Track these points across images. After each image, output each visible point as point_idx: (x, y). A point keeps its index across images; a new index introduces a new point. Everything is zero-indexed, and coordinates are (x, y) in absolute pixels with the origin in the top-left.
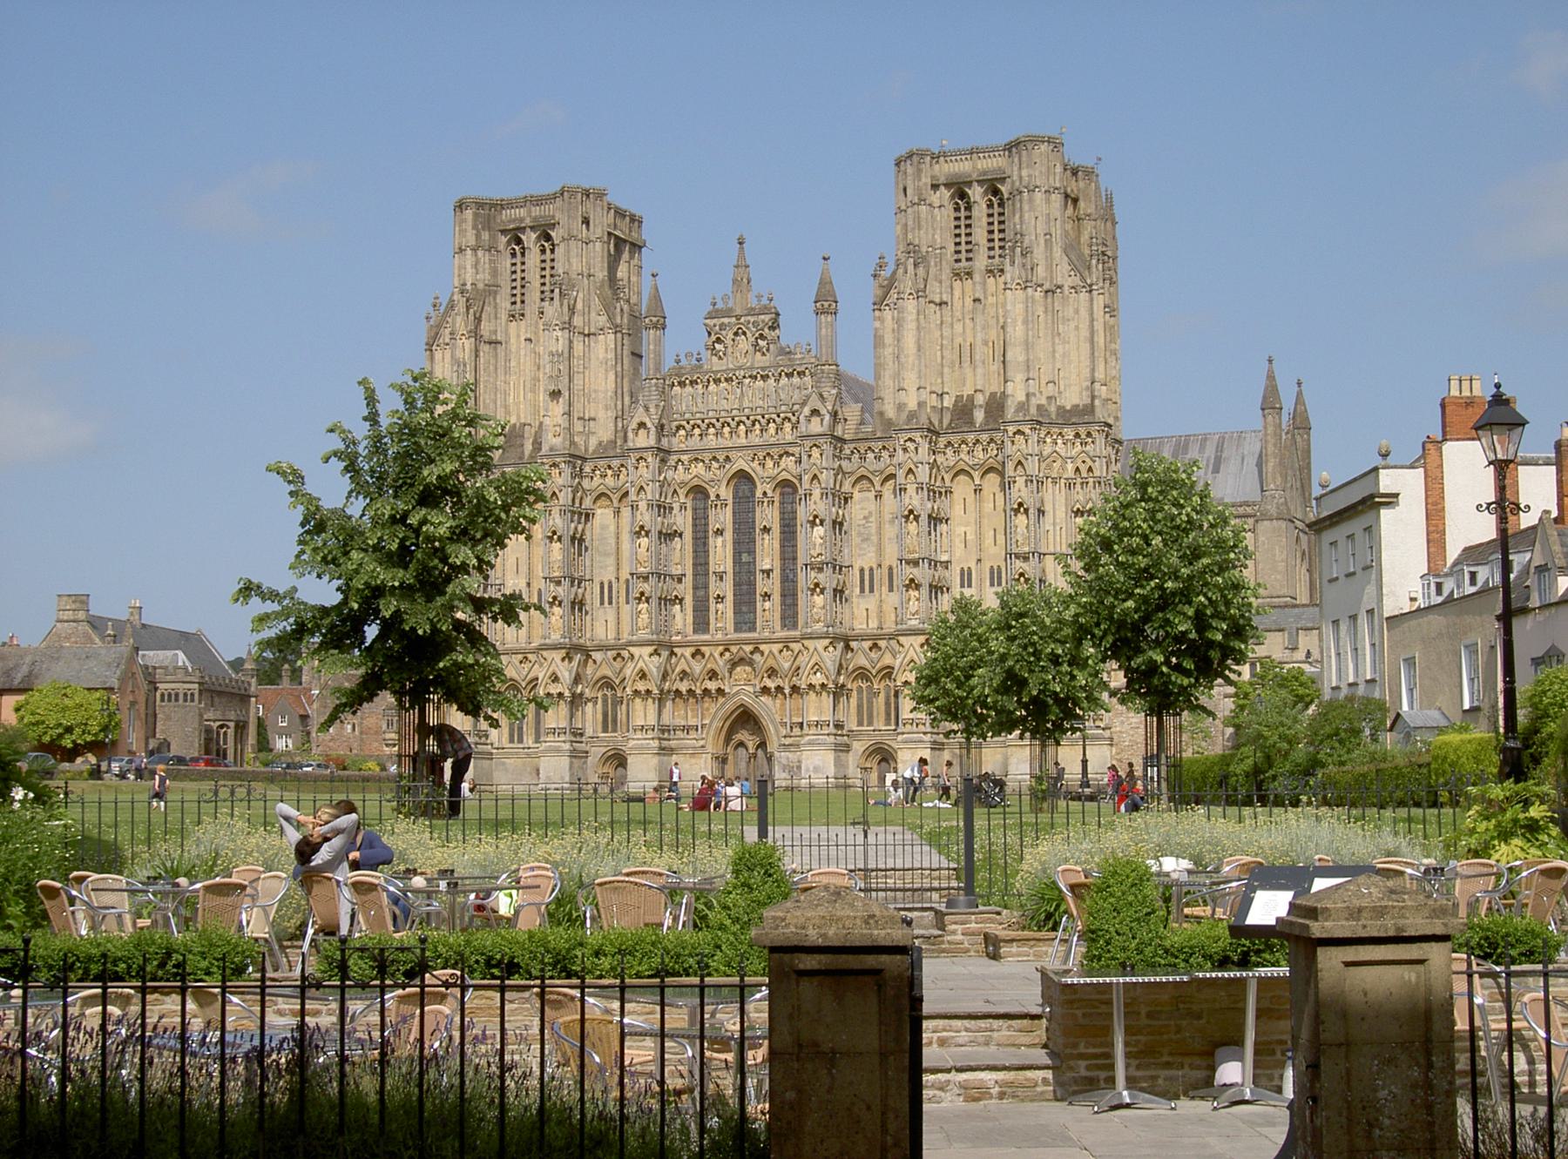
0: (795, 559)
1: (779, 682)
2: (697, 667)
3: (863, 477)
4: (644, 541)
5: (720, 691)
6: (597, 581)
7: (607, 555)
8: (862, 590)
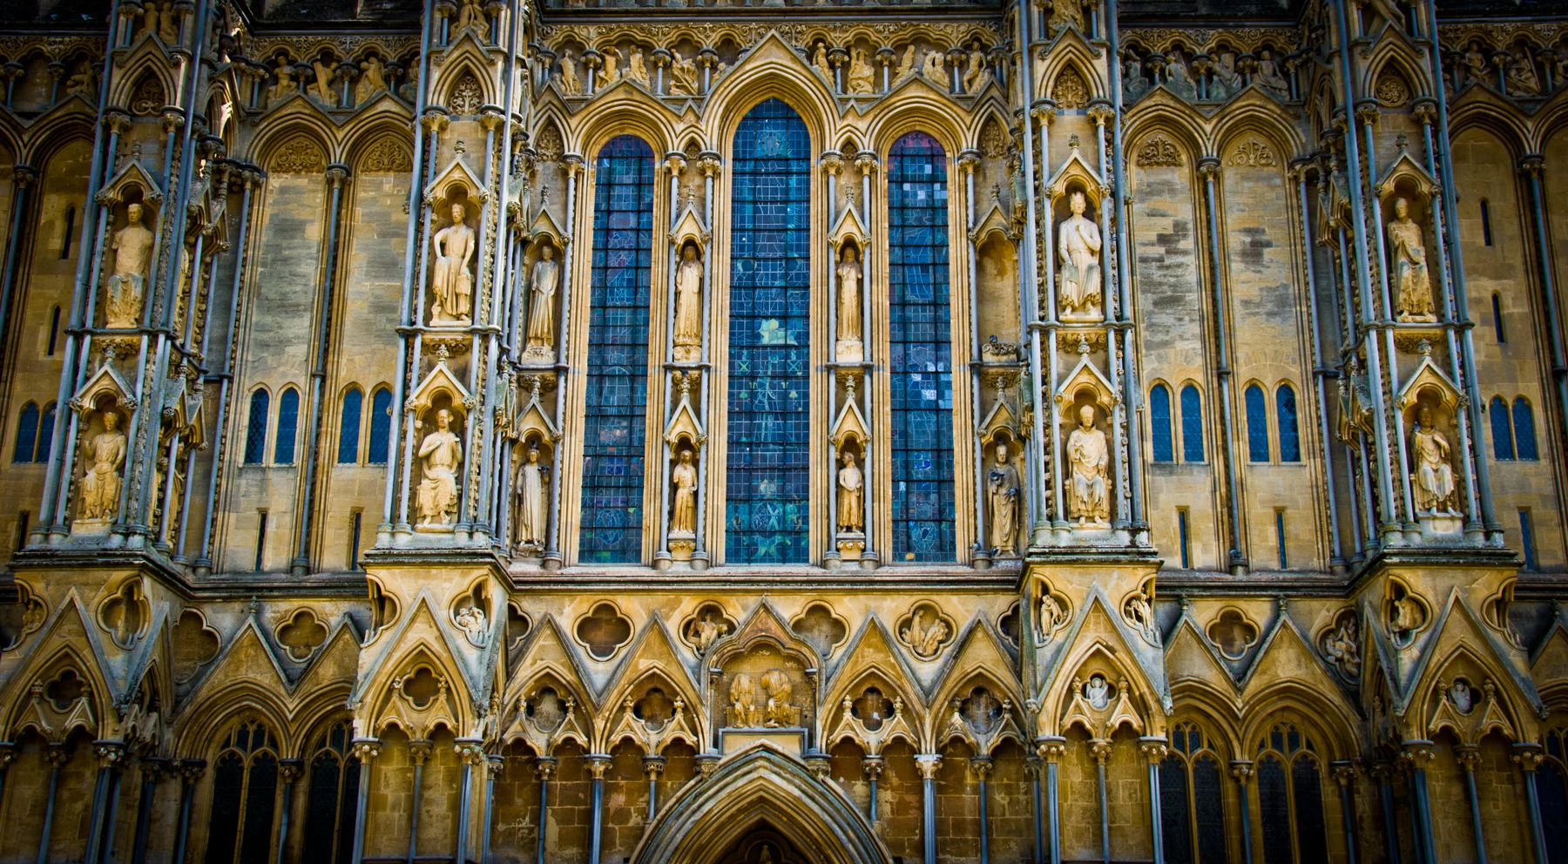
0: (940, 344)
1: (895, 727)
2: (598, 670)
3: (1162, 121)
4: (459, 238)
5: (682, 754)
6: (246, 385)
7: (286, 307)
8: (1163, 453)
